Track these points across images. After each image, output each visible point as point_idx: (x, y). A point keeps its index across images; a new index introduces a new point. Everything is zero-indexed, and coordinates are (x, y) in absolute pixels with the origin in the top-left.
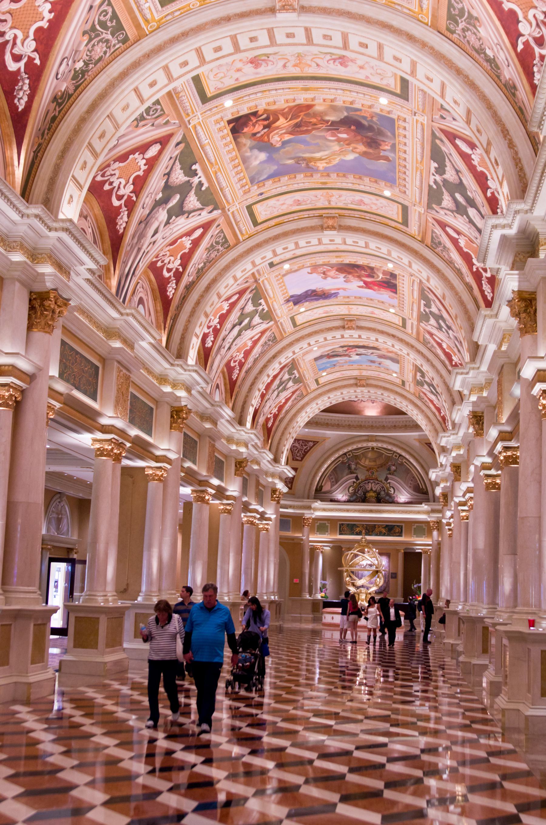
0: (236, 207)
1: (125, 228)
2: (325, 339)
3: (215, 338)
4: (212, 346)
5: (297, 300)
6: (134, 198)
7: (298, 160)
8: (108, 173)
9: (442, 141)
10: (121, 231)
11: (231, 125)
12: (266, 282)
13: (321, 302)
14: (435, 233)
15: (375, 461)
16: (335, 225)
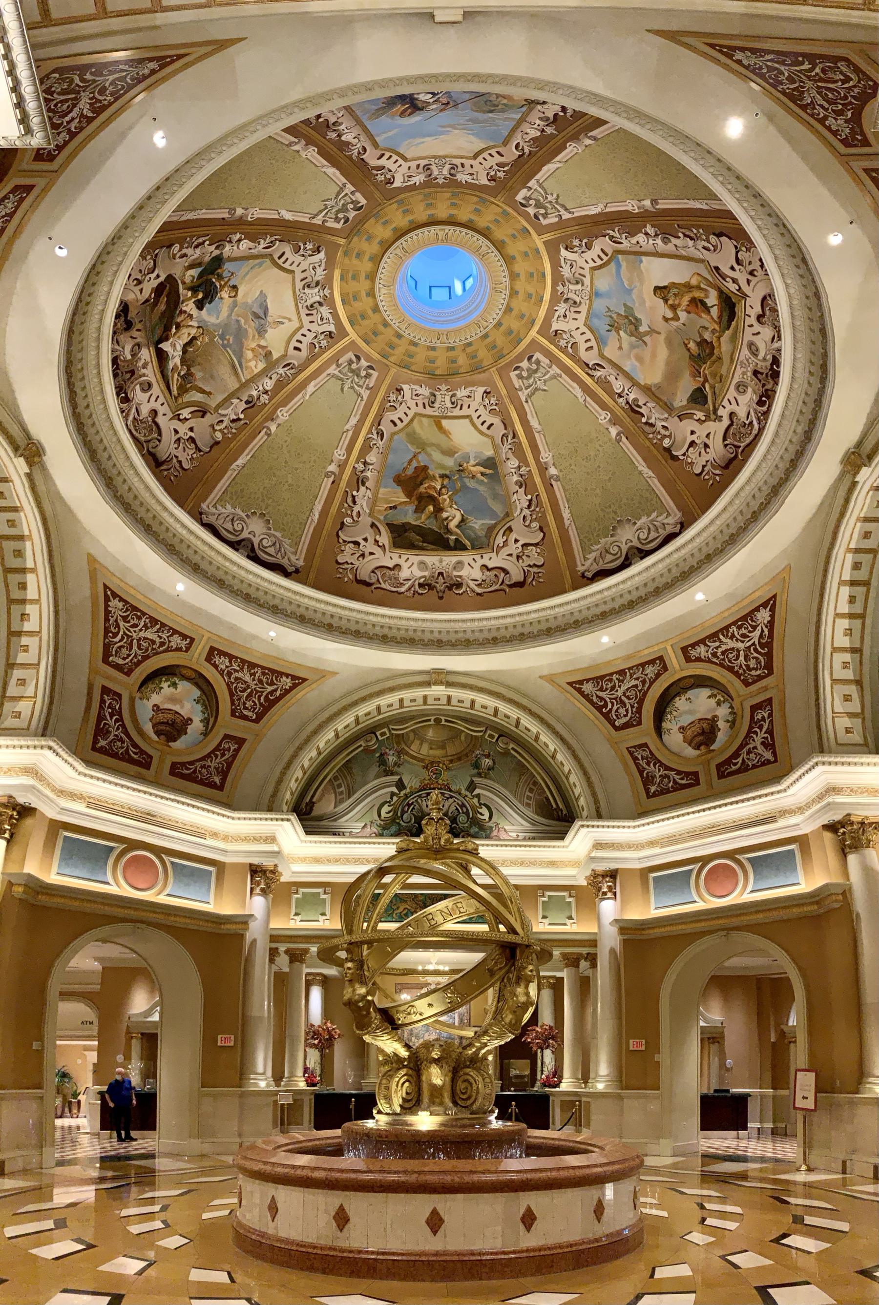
15: (443, 747)
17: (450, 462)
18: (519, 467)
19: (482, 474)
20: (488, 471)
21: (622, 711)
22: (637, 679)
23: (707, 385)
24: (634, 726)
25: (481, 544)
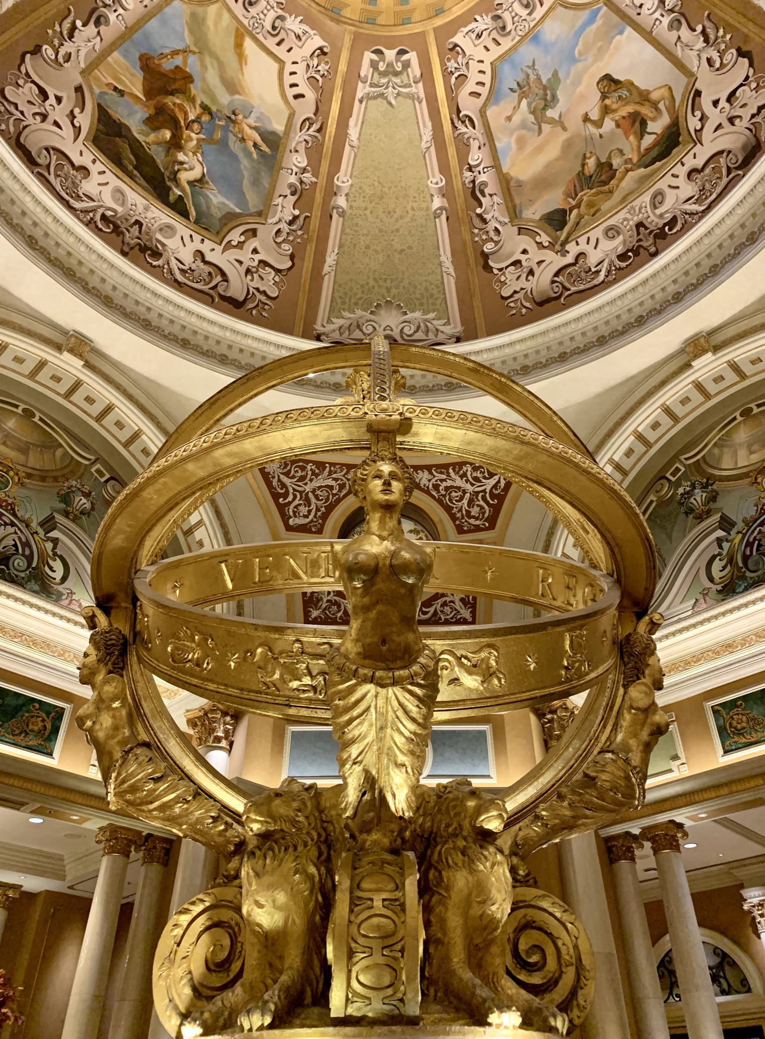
15: (24, 449)
17: (224, 99)
18: (304, 170)
19: (255, 145)
20: (264, 148)
21: (304, 510)
22: (336, 480)
23: (575, 212)
24: (311, 532)
25: (211, 226)
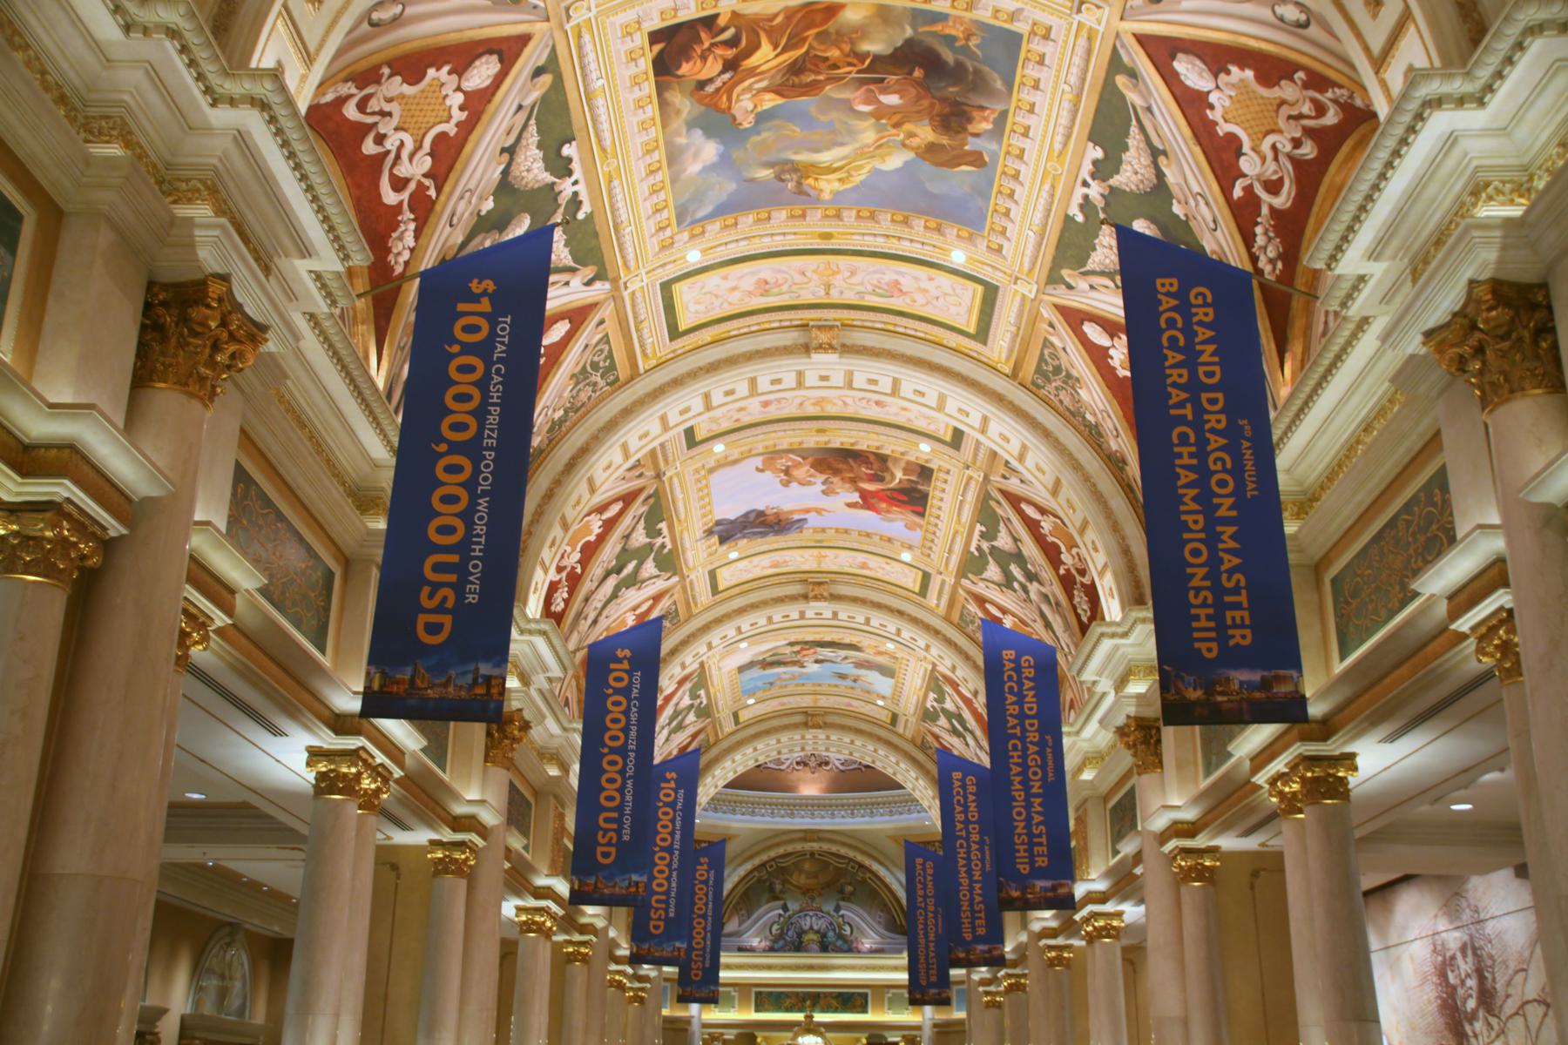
0: (641, 284)
1: (407, 263)
2: (770, 619)
3: (571, 593)
4: (564, 611)
5: (727, 532)
6: (432, 193)
7: (785, 168)
8: (374, 105)
9: (1133, 74)
10: (399, 269)
11: (658, 48)
12: (675, 480)
13: (773, 541)
14: (1053, 345)
15: (816, 877)
16: (834, 342)
